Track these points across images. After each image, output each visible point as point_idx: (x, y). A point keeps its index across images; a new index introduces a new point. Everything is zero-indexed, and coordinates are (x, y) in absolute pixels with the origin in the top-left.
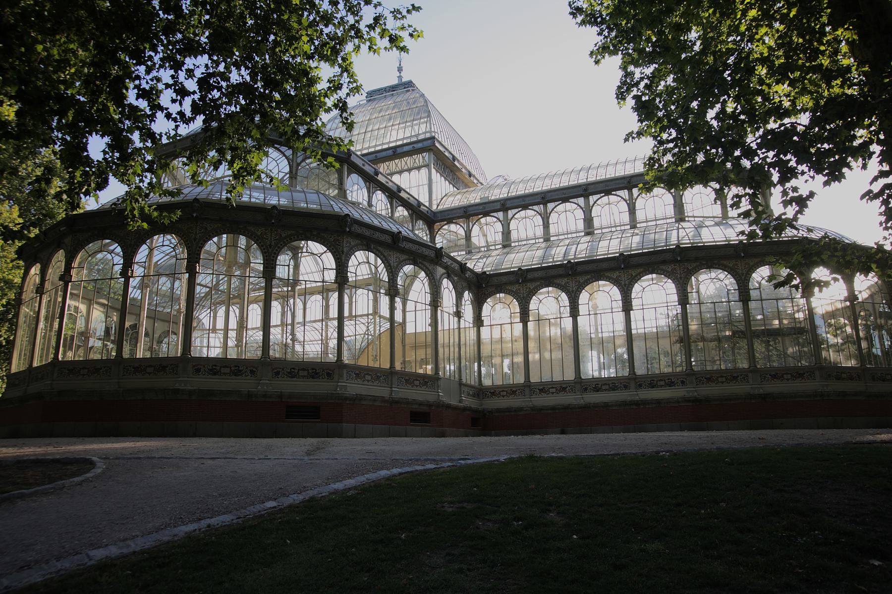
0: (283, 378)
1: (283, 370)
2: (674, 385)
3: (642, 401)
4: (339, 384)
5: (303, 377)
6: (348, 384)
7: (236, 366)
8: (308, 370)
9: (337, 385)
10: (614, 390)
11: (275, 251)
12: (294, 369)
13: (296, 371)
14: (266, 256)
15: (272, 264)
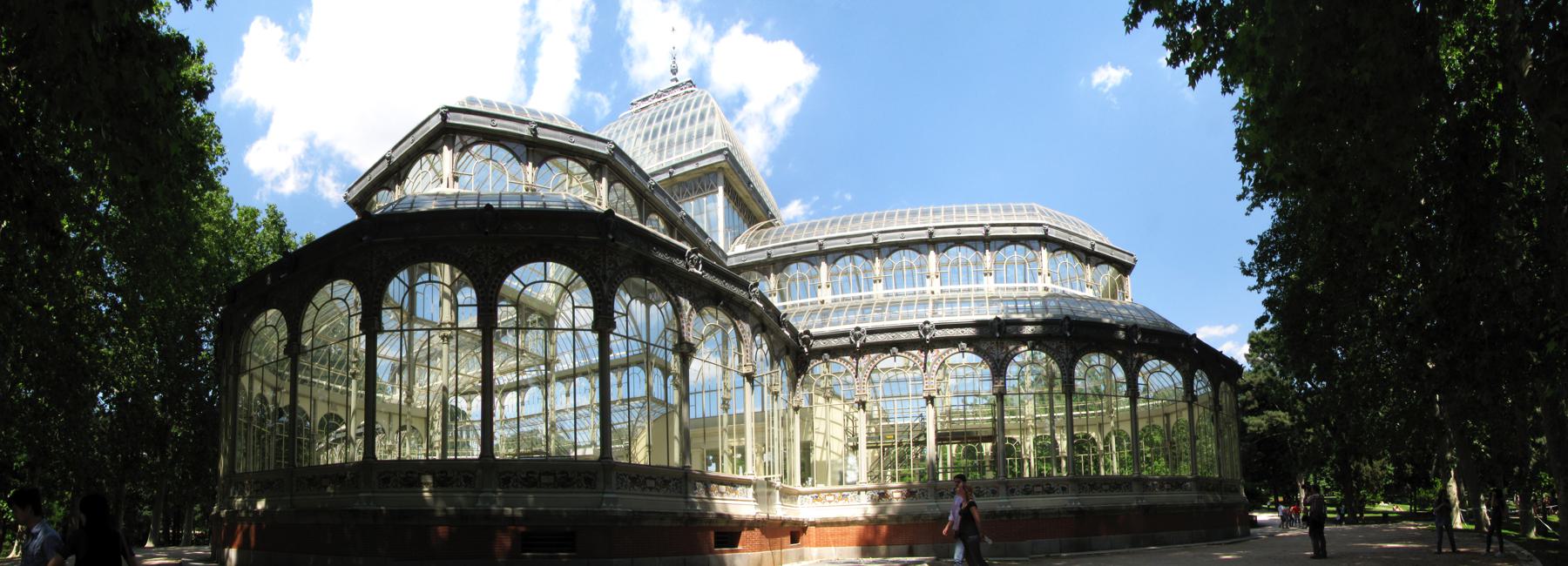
0: (517, 487)
1: (515, 475)
2: (1054, 492)
3: (1015, 511)
4: (606, 495)
5: (548, 485)
6: (619, 496)
7: (442, 472)
8: (555, 474)
9: (603, 498)
10: (1049, 493)
11: (493, 283)
12: (532, 472)
13: (536, 476)
14: (482, 292)
15: (491, 305)
